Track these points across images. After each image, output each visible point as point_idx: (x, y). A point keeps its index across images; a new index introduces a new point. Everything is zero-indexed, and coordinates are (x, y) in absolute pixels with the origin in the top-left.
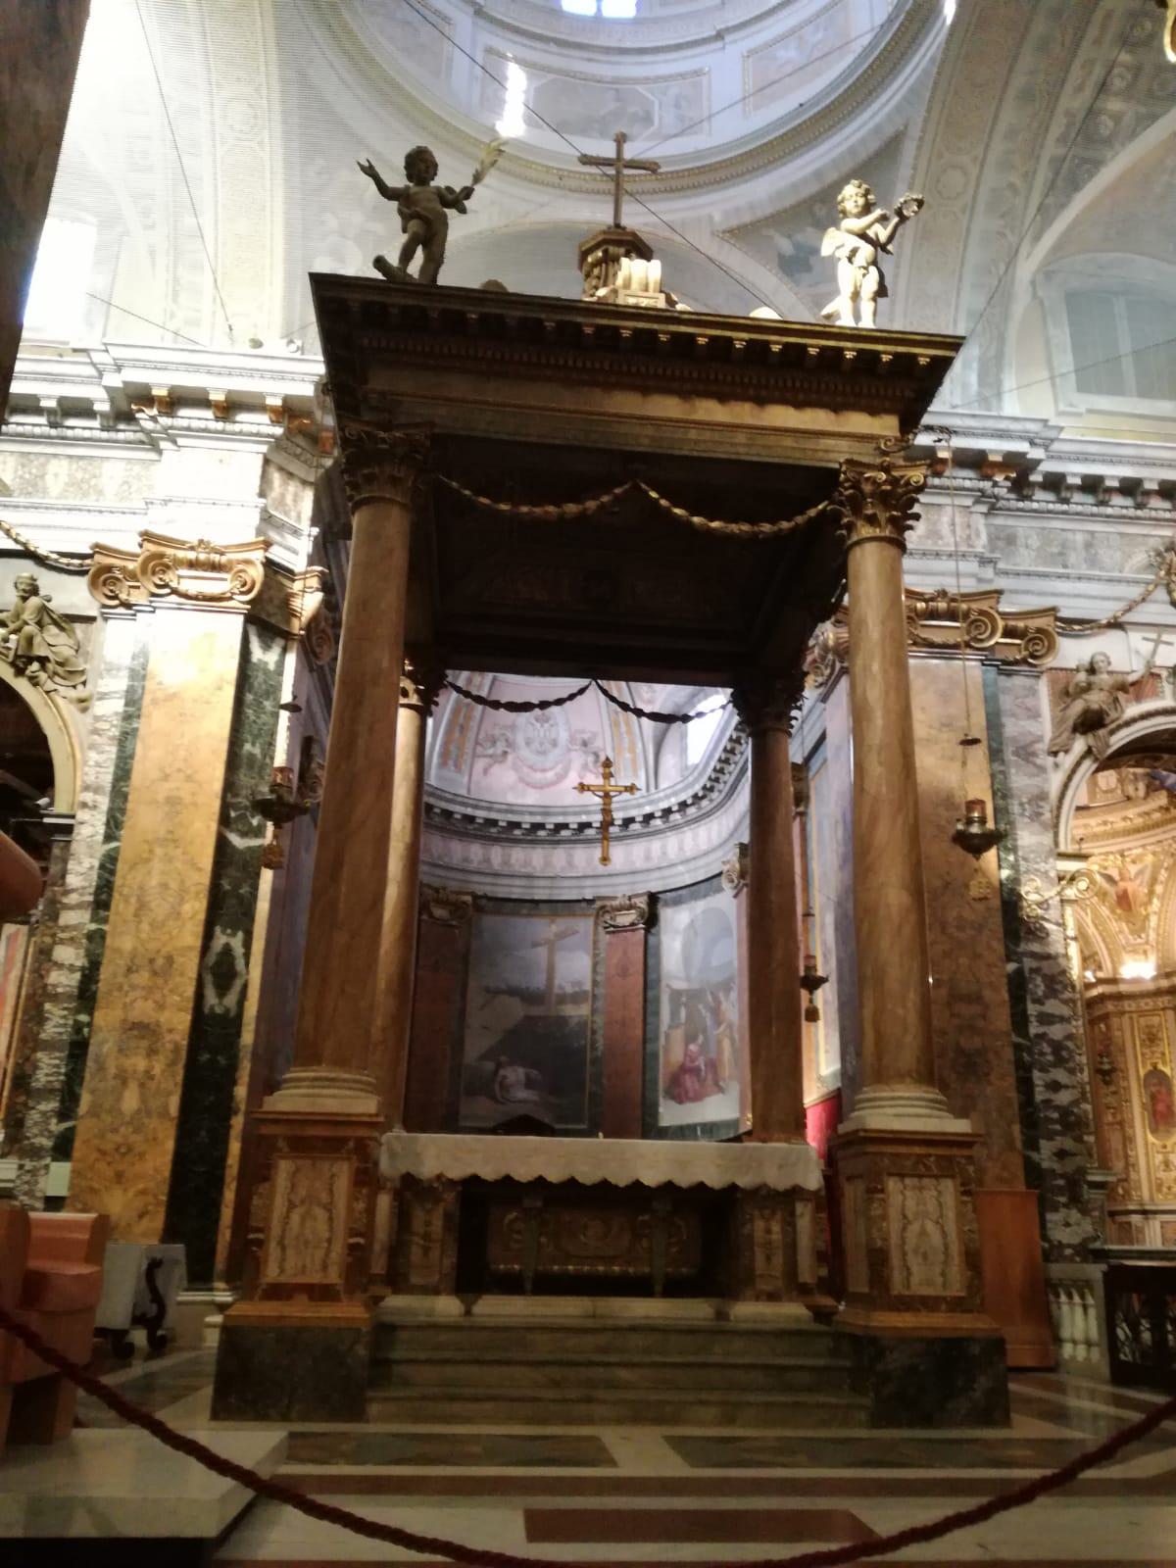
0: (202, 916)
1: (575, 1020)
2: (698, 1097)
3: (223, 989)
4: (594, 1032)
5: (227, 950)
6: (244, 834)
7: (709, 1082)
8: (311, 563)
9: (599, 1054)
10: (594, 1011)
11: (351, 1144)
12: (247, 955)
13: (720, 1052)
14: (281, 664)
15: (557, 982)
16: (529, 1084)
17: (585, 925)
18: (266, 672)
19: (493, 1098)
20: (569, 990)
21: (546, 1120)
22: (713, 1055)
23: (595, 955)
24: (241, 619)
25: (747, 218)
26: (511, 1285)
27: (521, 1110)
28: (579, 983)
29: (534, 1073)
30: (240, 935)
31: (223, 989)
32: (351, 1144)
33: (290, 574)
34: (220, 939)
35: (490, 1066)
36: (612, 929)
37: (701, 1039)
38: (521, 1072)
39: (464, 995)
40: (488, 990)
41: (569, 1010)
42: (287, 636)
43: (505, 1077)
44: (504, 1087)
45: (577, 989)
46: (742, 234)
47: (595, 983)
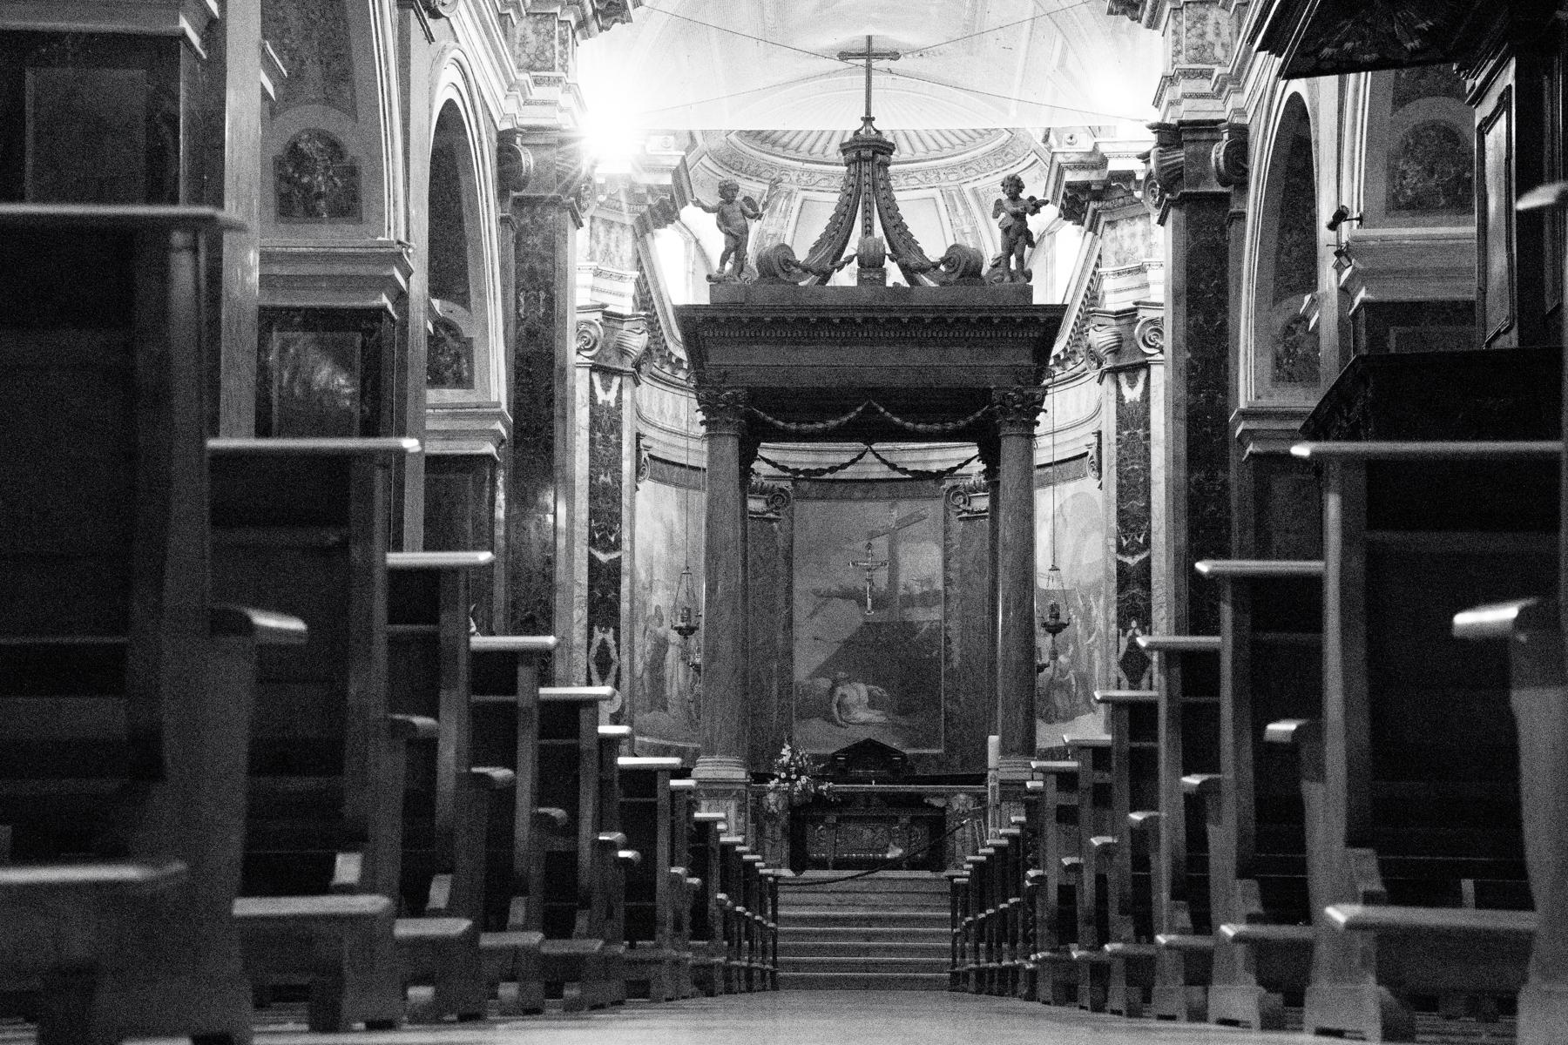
0: (585, 622)
1: (926, 626)
2: (1069, 717)
4: (948, 640)
5: (604, 642)
6: (605, 551)
7: (1080, 700)
9: (955, 665)
11: (734, 793)
12: (618, 646)
13: (1091, 663)
14: (619, 399)
15: (902, 579)
16: (873, 704)
17: (933, 509)
18: (609, 410)
19: (832, 721)
20: (917, 590)
21: (895, 745)
22: (1084, 669)
23: (946, 549)
24: (588, 371)
26: (821, 864)
27: (862, 735)
28: (929, 581)
29: (878, 690)
30: (611, 630)
32: (734, 793)
33: (621, 318)
34: (598, 636)
35: (825, 683)
36: (965, 515)
37: (1071, 648)
38: (862, 687)
39: (789, 602)
40: (816, 592)
41: (919, 615)
43: (843, 696)
45: (925, 589)
47: (948, 582)
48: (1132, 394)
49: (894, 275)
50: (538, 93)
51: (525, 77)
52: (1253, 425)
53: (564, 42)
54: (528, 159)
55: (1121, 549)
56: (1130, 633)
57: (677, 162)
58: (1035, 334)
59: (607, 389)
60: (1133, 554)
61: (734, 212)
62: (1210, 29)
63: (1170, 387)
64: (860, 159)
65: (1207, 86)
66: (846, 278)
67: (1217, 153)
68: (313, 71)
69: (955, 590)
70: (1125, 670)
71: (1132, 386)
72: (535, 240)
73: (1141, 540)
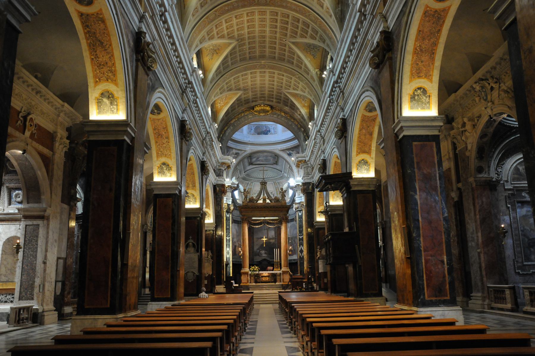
3: (228, 254)
5: (228, 250)
8: (232, 203)
10: (275, 241)
14: (230, 216)
15: (269, 236)
16: (265, 253)
19: (260, 256)
20: (271, 237)
21: (268, 259)
25: (283, 149)
26: (259, 282)
27: (264, 258)
28: (273, 236)
31: (228, 254)
33: (230, 205)
34: (227, 249)
35: (258, 251)
40: (257, 238)
42: (230, 212)
44: (261, 254)
46: (283, 150)
47: (275, 236)
48: (300, 214)
49: (268, 201)
50: (219, 179)
51: (217, 178)
52: (316, 224)
53: (222, 172)
54: (218, 189)
57: (237, 183)
58: (287, 209)
59: (228, 214)
61: (245, 193)
62: (309, 170)
63: (306, 213)
64: (262, 184)
65: (309, 178)
66: (261, 201)
67: (310, 187)
68: (191, 185)
69: (276, 237)
71: (300, 213)
72: (219, 199)
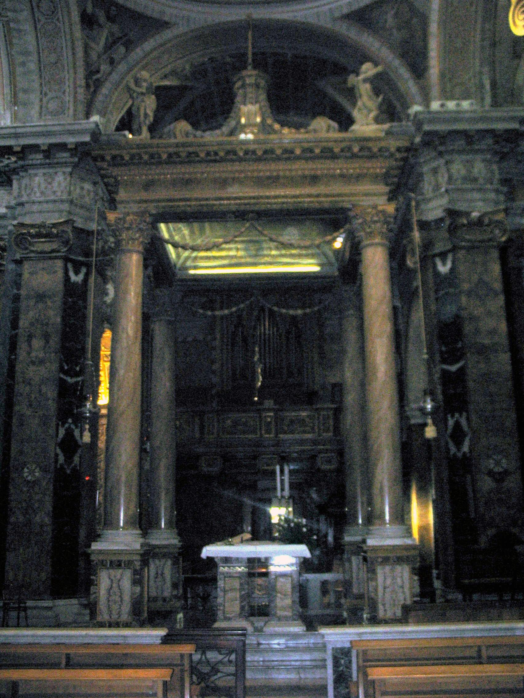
55: (62, 370)
56: (67, 425)
60: (72, 377)
70: (63, 450)
73: (78, 369)
